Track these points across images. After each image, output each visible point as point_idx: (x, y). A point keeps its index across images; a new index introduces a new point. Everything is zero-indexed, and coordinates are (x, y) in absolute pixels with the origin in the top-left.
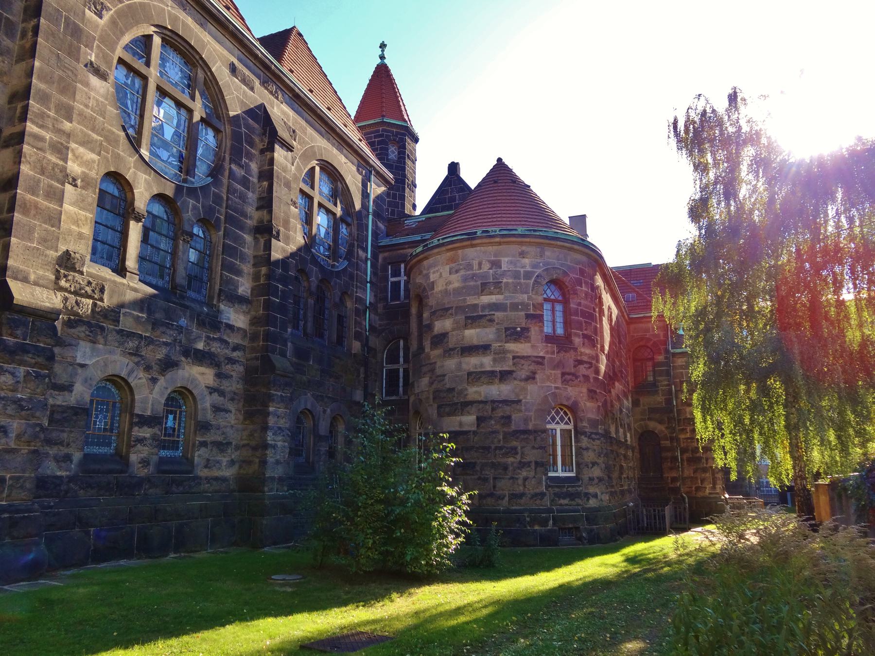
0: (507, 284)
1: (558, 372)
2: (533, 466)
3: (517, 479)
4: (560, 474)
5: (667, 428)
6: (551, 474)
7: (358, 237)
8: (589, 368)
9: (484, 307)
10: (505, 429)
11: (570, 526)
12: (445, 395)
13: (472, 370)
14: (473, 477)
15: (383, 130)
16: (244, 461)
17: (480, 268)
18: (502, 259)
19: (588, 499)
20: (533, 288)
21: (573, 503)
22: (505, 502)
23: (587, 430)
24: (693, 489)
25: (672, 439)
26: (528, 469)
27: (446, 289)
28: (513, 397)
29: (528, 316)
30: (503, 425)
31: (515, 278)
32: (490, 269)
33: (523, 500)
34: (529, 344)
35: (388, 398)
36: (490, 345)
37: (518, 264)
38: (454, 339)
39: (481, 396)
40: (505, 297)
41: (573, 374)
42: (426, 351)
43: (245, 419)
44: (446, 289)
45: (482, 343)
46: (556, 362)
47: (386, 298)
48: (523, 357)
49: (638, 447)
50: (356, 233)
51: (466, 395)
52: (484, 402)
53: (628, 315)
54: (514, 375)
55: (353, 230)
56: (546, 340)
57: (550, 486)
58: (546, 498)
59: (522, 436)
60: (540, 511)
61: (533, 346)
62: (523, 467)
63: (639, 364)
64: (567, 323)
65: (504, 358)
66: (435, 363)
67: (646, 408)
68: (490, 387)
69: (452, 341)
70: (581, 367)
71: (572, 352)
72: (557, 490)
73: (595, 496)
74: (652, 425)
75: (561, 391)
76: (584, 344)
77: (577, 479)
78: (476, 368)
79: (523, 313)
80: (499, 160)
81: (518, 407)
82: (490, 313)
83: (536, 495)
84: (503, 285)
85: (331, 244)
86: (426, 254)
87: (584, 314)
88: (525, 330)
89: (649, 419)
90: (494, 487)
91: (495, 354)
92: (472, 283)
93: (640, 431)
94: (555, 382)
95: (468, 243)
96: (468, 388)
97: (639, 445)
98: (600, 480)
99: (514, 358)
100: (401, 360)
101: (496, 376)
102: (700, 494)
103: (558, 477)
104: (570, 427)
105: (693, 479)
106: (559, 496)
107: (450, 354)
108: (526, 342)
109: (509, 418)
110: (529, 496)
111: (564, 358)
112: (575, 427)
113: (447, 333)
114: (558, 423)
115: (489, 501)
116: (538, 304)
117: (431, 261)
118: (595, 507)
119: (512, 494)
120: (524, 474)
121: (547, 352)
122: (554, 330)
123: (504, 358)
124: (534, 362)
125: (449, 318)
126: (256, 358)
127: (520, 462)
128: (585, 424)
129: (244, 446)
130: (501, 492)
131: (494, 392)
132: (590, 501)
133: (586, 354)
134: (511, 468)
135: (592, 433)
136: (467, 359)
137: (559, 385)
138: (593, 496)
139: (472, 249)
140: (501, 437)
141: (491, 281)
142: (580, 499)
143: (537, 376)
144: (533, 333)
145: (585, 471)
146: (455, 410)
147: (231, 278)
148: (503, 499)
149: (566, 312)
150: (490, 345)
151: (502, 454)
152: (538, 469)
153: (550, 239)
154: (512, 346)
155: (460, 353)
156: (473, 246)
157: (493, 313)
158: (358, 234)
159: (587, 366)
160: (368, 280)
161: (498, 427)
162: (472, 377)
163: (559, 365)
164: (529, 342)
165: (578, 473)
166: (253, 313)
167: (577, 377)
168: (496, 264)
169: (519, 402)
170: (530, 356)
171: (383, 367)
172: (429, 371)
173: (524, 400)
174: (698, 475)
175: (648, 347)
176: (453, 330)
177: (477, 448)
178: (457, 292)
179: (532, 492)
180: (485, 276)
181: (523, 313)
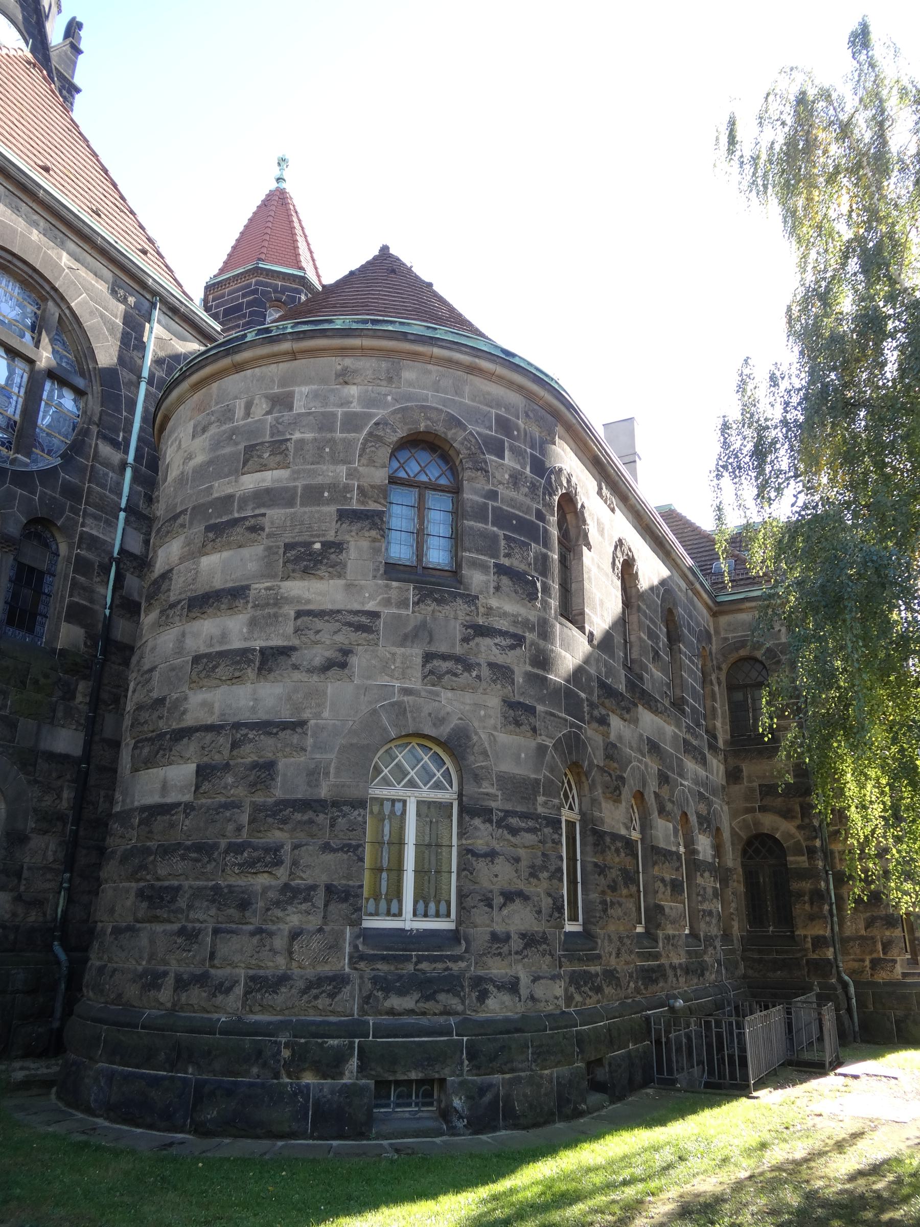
0: (302, 441)
1: (415, 653)
2: (319, 898)
3: (271, 934)
4: (409, 922)
5: (799, 827)
6: (371, 923)
7: (100, 419)
8: (512, 647)
9: (244, 501)
10: (259, 798)
11: (413, 1075)
13: (203, 650)
14: (168, 927)
15: (257, 283)
17: (248, 414)
19: (483, 996)
20: (363, 450)
21: (429, 1005)
22: (233, 1001)
23: (493, 805)
24: (867, 963)
25: (811, 851)
26: (304, 907)
28: (286, 715)
29: (344, 516)
30: (254, 786)
31: (321, 429)
32: (268, 413)
33: (281, 998)
34: (341, 582)
36: (248, 587)
37: (332, 399)
39: (212, 713)
40: (294, 472)
41: (458, 659)
45: (230, 585)
46: (410, 628)
48: (320, 614)
49: (740, 870)
50: (98, 409)
51: (184, 712)
53: (713, 599)
54: (295, 658)
56: (385, 572)
57: (362, 957)
58: (347, 990)
59: (298, 816)
60: (323, 1031)
61: (349, 587)
62: (290, 902)
63: (739, 696)
64: (457, 539)
65: (276, 616)
67: (755, 784)
69: (177, 588)
70: (485, 643)
71: (461, 607)
72: (383, 967)
73: (513, 987)
74: (770, 822)
75: (420, 700)
76: (497, 588)
77: (454, 937)
78: (211, 646)
80: (385, 249)
81: (295, 739)
82: (257, 512)
83: (320, 981)
84: (291, 446)
85: (17, 418)
87: (502, 519)
88: (338, 546)
89: (763, 809)
90: (212, 956)
91: (255, 606)
92: (228, 450)
93: (744, 835)
94: (404, 676)
95: (226, 362)
96: (190, 694)
97: (743, 865)
98: (531, 941)
99: (299, 614)
101: (250, 662)
102: (882, 976)
103: (400, 933)
104: (448, 795)
105: (866, 941)
106: (386, 985)
109: (270, 766)
110: (301, 984)
111: (434, 619)
112: (460, 795)
114: (412, 784)
115: (196, 996)
116: (373, 487)
118: (507, 1020)
119: (253, 978)
120: (294, 918)
121: (387, 602)
122: (420, 552)
124: (349, 624)
127: (286, 886)
128: (487, 788)
130: (228, 970)
132: (491, 1003)
133: (505, 615)
134: (261, 904)
135: (508, 813)
137: (415, 682)
138: (499, 988)
139: (236, 377)
140: (245, 818)
141: (268, 439)
142: (456, 995)
143: (354, 660)
145: (480, 915)
148: (228, 990)
149: (457, 513)
150: (248, 587)
151: (240, 865)
152: (331, 907)
153: (413, 341)
156: (238, 368)
157: (262, 511)
158: (102, 412)
159: (509, 641)
160: (123, 505)
161: (240, 792)
163: (421, 633)
164: (340, 576)
165: (459, 922)
167: (468, 667)
168: (282, 402)
169: (302, 723)
170: (339, 611)
173: (312, 722)
174: (876, 932)
175: (756, 660)
176: (182, 559)
177: (188, 849)
178: (201, 473)
179: (310, 973)
181: (332, 509)
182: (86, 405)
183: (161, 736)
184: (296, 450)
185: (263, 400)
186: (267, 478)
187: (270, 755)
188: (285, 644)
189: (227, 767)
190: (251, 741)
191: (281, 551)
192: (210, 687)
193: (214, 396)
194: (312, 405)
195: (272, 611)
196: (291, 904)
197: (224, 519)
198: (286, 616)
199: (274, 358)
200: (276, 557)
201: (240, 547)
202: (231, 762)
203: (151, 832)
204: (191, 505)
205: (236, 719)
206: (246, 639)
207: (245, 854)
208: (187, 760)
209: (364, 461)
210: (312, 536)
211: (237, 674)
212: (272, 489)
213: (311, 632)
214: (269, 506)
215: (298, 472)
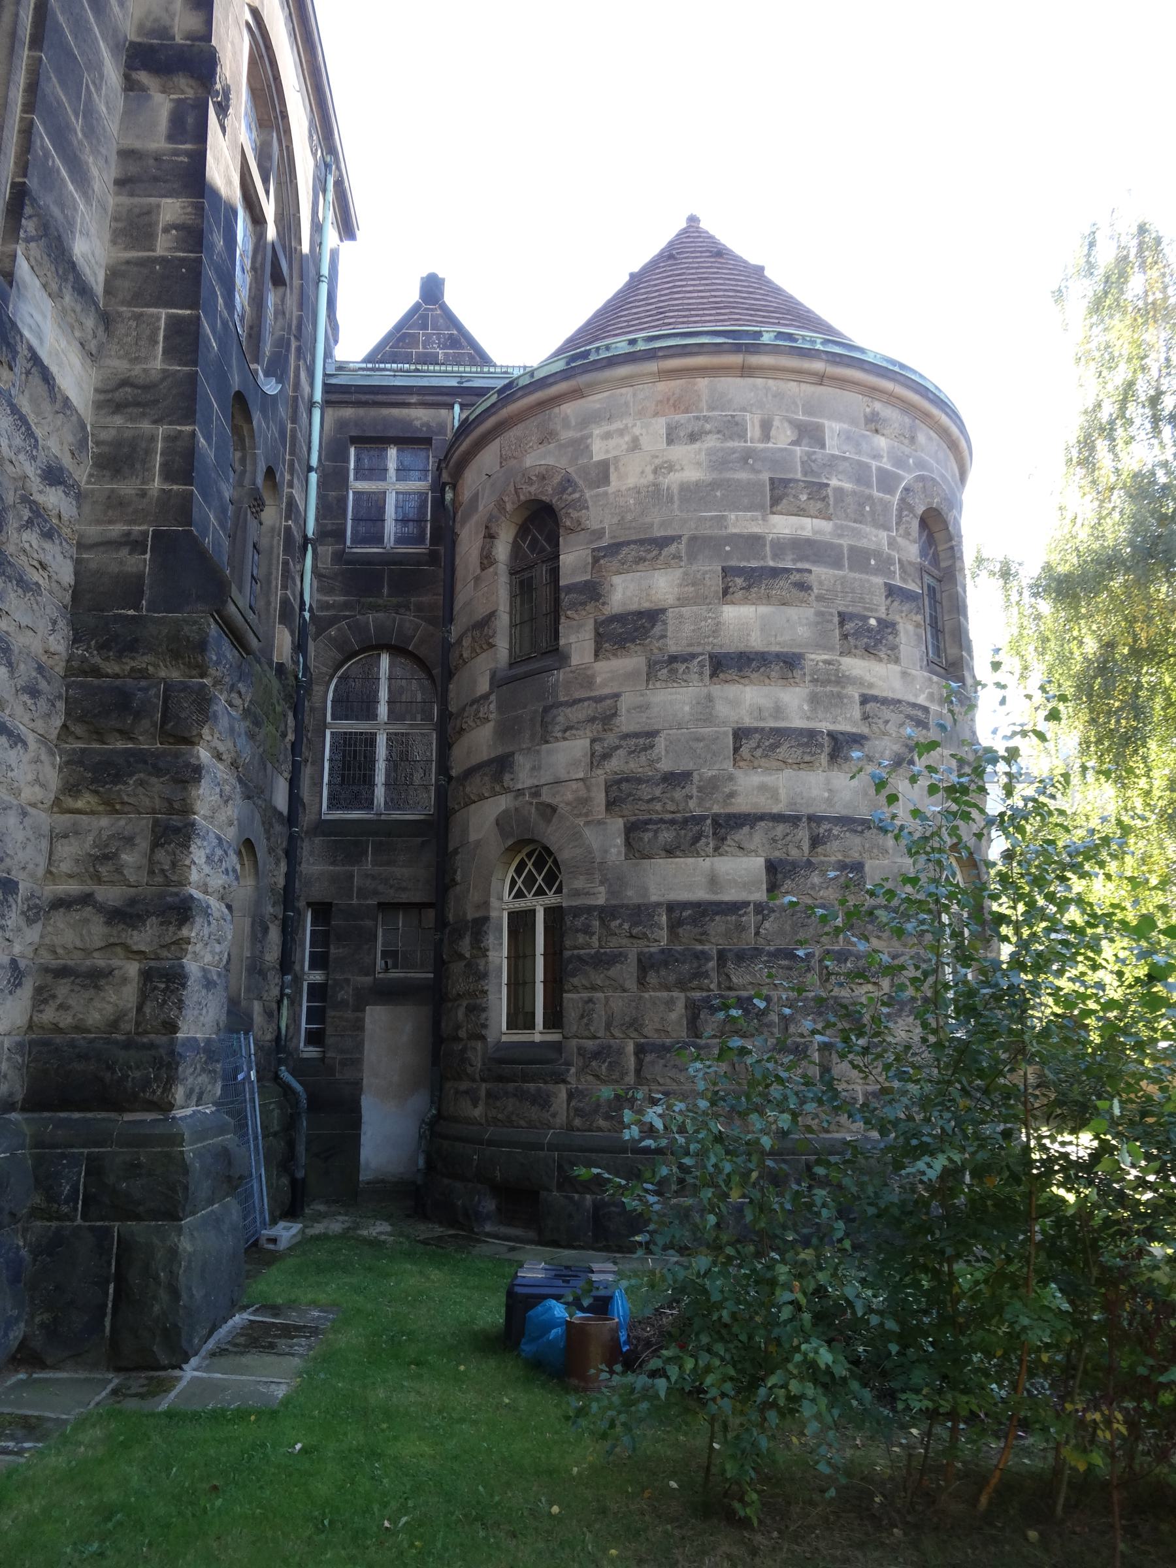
0: (839, 491)
9: (781, 547)
12: (658, 792)
13: (748, 722)
16: (62, 972)
18: (826, 423)
20: (900, 517)
27: (656, 485)
32: (793, 443)
34: (897, 668)
35: (338, 815)
38: (688, 629)
39: (777, 801)
42: (575, 660)
43: (71, 788)
44: (656, 485)
47: (339, 534)
48: (885, 701)
51: (732, 795)
52: (793, 820)
55: (288, 302)
61: (904, 674)
66: (617, 696)
68: (802, 773)
78: (762, 719)
79: (879, 581)
80: (693, 220)
82: (799, 565)
84: (830, 491)
86: (582, 380)
88: (887, 626)
91: (814, 681)
92: (743, 475)
95: (736, 359)
96: (738, 773)
99: (865, 700)
100: (383, 710)
107: (673, 672)
108: (889, 662)
109: (858, 867)
113: (663, 611)
117: (594, 402)
123: (840, 696)
125: (667, 565)
126: (136, 545)
129: (61, 903)
131: (815, 793)
136: (732, 690)
141: (799, 476)
144: (902, 635)
146: (696, 839)
147: (58, 171)
153: (931, 401)
154: (856, 666)
155: (707, 671)
156: (746, 371)
157: (807, 566)
162: (753, 743)
164: (897, 661)
166: (120, 366)
168: (809, 433)
170: (899, 701)
171: (325, 726)
172: (592, 720)
176: (682, 601)
177: (769, 954)
178: (692, 493)
180: (777, 460)
181: (879, 581)
182: (283, 300)
183: (699, 820)
184: (836, 503)
185: (786, 425)
186: (808, 527)
187: (856, 855)
188: (854, 730)
189: (809, 864)
190: (837, 837)
191: (836, 620)
192: (767, 769)
193: (704, 398)
194: (845, 448)
195: (835, 690)
196: (900, 1016)
197: (754, 564)
198: (850, 697)
199: (799, 375)
200: (831, 626)
201: (784, 604)
202: (813, 859)
203: (704, 933)
204: (687, 533)
205: (811, 811)
206: (808, 718)
207: (849, 965)
208: (756, 853)
209: (901, 531)
210: (866, 609)
211: (807, 758)
212: (815, 541)
213: (880, 721)
214: (814, 562)
215: (842, 527)
